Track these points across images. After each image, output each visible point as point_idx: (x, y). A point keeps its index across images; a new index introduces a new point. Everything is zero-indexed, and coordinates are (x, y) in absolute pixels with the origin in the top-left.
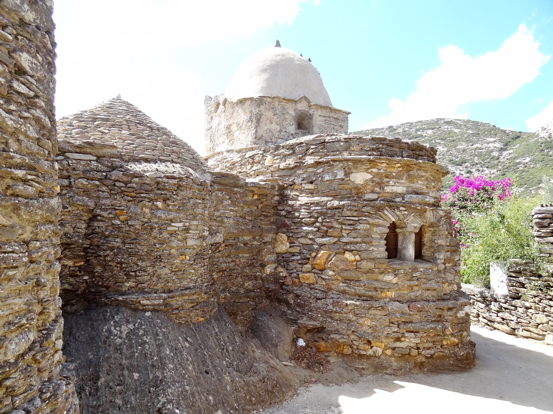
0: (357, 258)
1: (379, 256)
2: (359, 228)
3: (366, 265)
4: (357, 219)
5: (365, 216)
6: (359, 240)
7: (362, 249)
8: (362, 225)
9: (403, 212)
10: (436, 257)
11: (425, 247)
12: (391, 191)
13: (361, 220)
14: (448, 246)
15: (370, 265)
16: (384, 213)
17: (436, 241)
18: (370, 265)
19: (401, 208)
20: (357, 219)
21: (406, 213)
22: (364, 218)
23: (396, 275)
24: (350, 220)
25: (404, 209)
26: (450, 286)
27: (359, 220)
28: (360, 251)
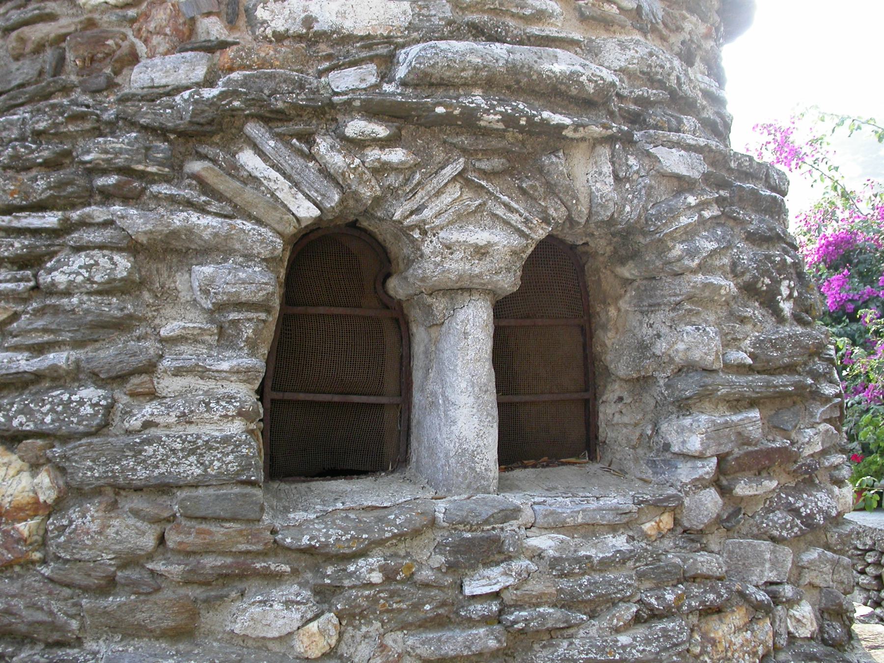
0: (44, 486)
1: (191, 469)
2: (61, 278)
3: (108, 532)
4: (51, 219)
5: (107, 196)
6: (59, 358)
7: (74, 424)
8: (81, 259)
9: (374, 154)
10: (667, 447)
11: (613, 392)
12: (297, 28)
13: (84, 224)
14: (741, 369)
15: (129, 531)
16: (234, 170)
17: (661, 347)
18: (129, 531)
19: (356, 127)
20: (51, 219)
21: (396, 155)
22: (98, 213)
23: (324, 595)
24: (20, 232)
25: (381, 131)
26: (765, 628)
27: (66, 228)
28: (66, 439)
